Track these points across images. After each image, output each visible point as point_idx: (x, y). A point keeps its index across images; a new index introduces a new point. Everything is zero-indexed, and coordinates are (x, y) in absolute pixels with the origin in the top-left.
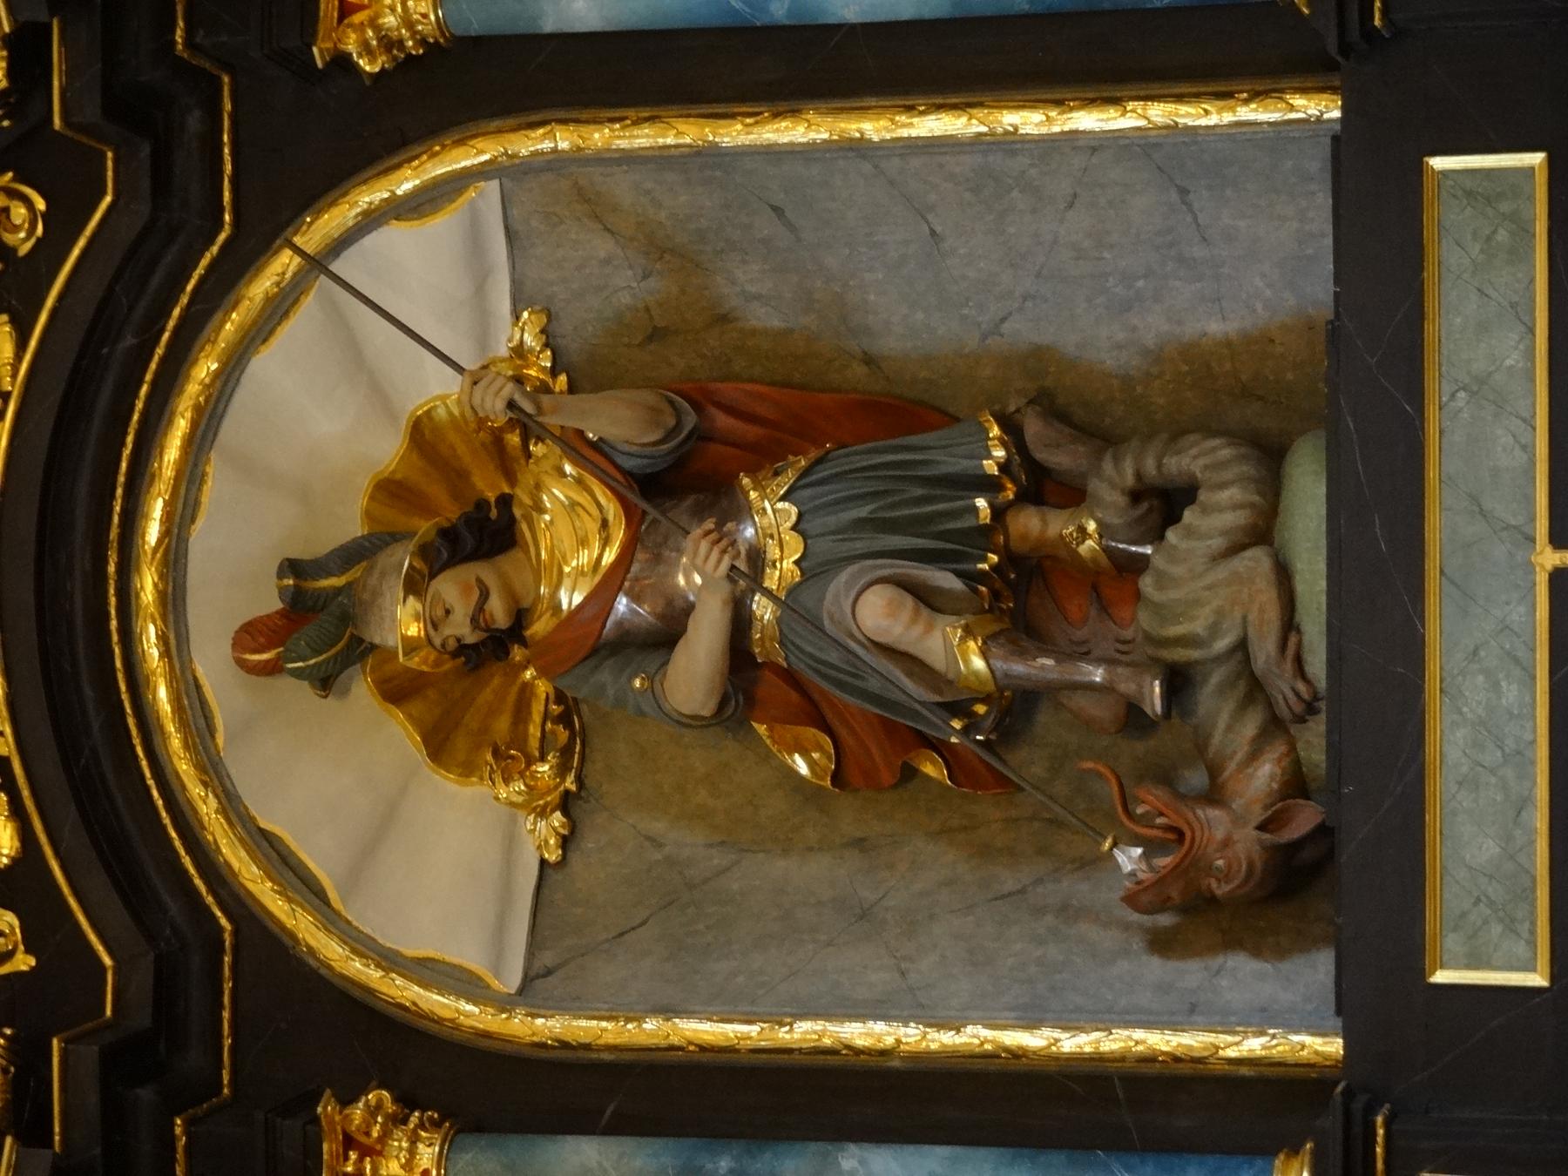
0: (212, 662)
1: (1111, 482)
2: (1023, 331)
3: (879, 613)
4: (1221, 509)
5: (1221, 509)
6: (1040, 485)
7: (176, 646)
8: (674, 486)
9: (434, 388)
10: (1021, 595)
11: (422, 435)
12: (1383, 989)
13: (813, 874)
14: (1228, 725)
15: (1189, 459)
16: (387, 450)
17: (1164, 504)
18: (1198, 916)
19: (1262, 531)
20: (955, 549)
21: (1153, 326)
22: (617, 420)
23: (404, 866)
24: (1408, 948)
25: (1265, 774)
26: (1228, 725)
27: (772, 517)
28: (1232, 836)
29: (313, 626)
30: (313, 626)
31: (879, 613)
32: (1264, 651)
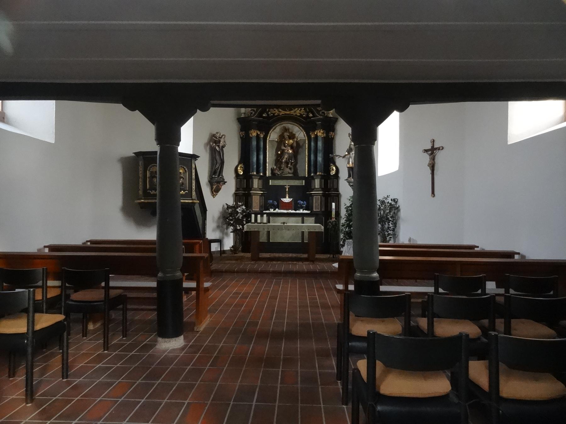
1: (292, 167)
3: (286, 157)
4: (290, 171)
5: (290, 171)
6: (292, 163)
8: (292, 147)
9: (297, 135)
10: (287, 163)
11: (294, 135)
12: (269, 178)
13: (274, 153)
14: (281, 172)
15: (293, 170)
16: (294, 133)
17: (290, 169)
18: (272, 170)
19: (289, 173)
20: (289, 160)
21: (299, 168)
22: (295, 145)
23: (274, 136)
26: (281, 172)
27: (291, 152)
28: (276, 172)
29: (286, 130)
31: (286, 157)
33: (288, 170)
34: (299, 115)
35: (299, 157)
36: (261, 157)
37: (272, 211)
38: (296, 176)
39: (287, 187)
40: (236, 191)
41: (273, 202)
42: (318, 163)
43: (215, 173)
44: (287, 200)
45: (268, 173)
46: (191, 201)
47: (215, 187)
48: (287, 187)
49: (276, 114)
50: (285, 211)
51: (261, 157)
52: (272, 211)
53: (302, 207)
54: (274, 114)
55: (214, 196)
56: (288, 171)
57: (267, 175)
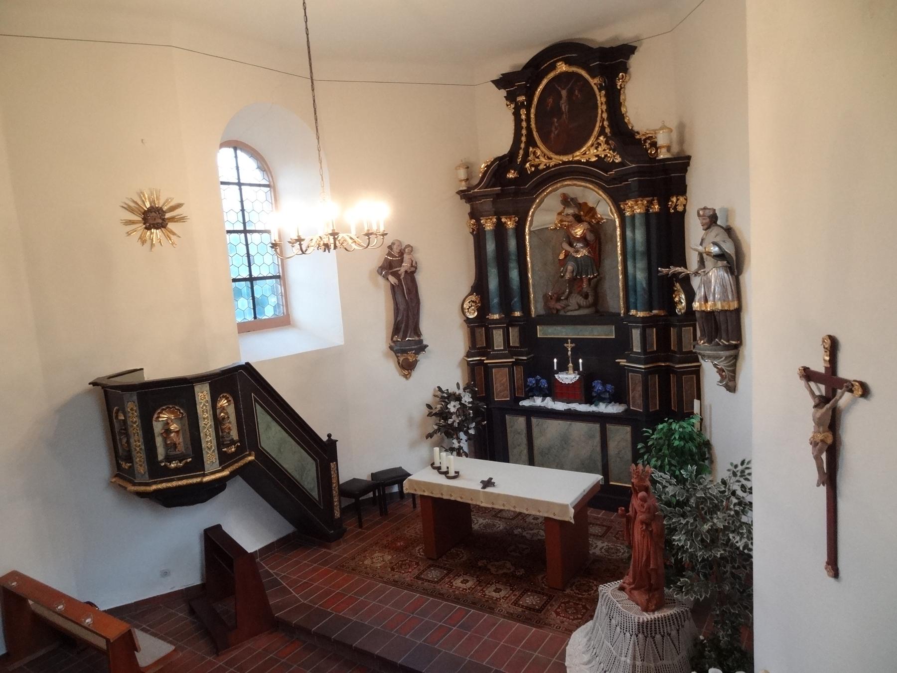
0: (561, 191)
2: (607, 277)
7: (560, 187)
15: (591, 299)
16: (591, 205)
17: (586, 297)
19: (580, 307)
21: (608, 292)
24: (540, 324)
25: (559, 307)
29: (567, 201)
30: (567, 201)
32: (569, 308)
33: (576, 300)
34: (594, 159)
35: (607, 263)
36: (514, 274)
37: (538, 402)
38: (599, 314)
39: (569, 346)
40: (469, 355)
41: (538, 381)
42: (639, 289)
43: (396, 330)
44: (568, 378)
45: (535, 309)
46: (199, 480)
47: (401, 359)
48: (569, 346)
49: (542, 167)
50: (560, 406)
51: (514, 274)
52: (538, 402)
53: (602, 400)
54: (536, 166)
55: (407, 377)
56: (575, 304)
57: (501, 332)
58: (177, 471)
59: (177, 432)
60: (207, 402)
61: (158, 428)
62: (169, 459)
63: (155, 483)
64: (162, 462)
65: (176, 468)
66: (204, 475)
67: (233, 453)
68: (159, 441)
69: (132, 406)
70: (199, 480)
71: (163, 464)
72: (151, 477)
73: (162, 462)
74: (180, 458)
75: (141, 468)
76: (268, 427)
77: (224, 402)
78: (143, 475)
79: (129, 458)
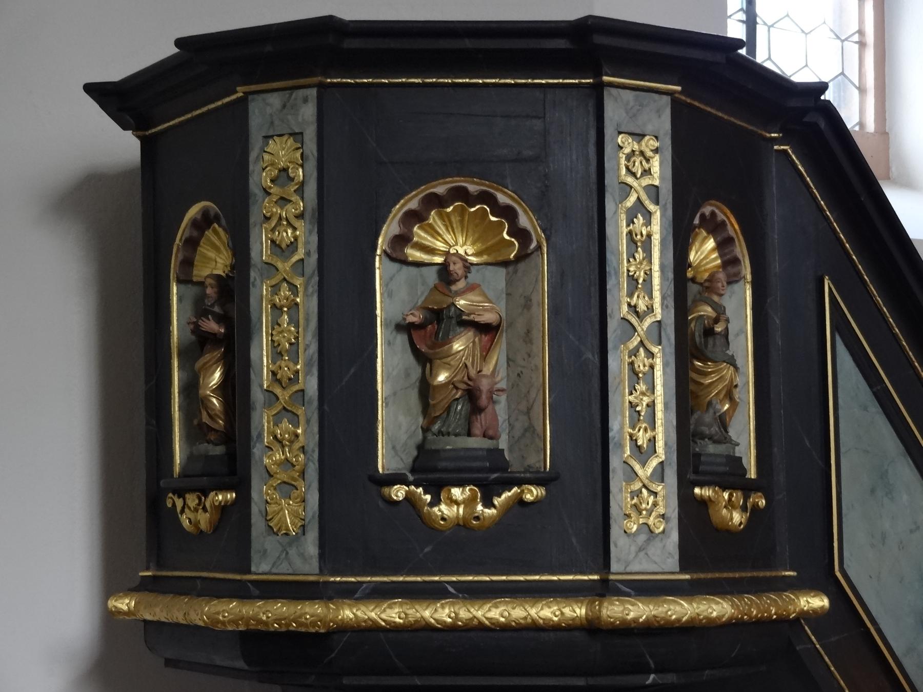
46: (577, 611)
58: (463, 548)
59: (488, 330)
60: (654, 192)
61: (391, 295)
62: (433, 471)
63: (349, 593)
64: (396, 479)
65: (462, 527)
66: (606, 589)
67: (727, 533)
68: (389, 359)
69: (283, 147)
70: (577, 611)
71: (399, 492)
72: (330, 556)
73: (396, 479)
74: (490, 476)
75: (286, 508)
76: (882, 484)
77: (704, 252)
78: (293, 540)
79: (229, 460)
